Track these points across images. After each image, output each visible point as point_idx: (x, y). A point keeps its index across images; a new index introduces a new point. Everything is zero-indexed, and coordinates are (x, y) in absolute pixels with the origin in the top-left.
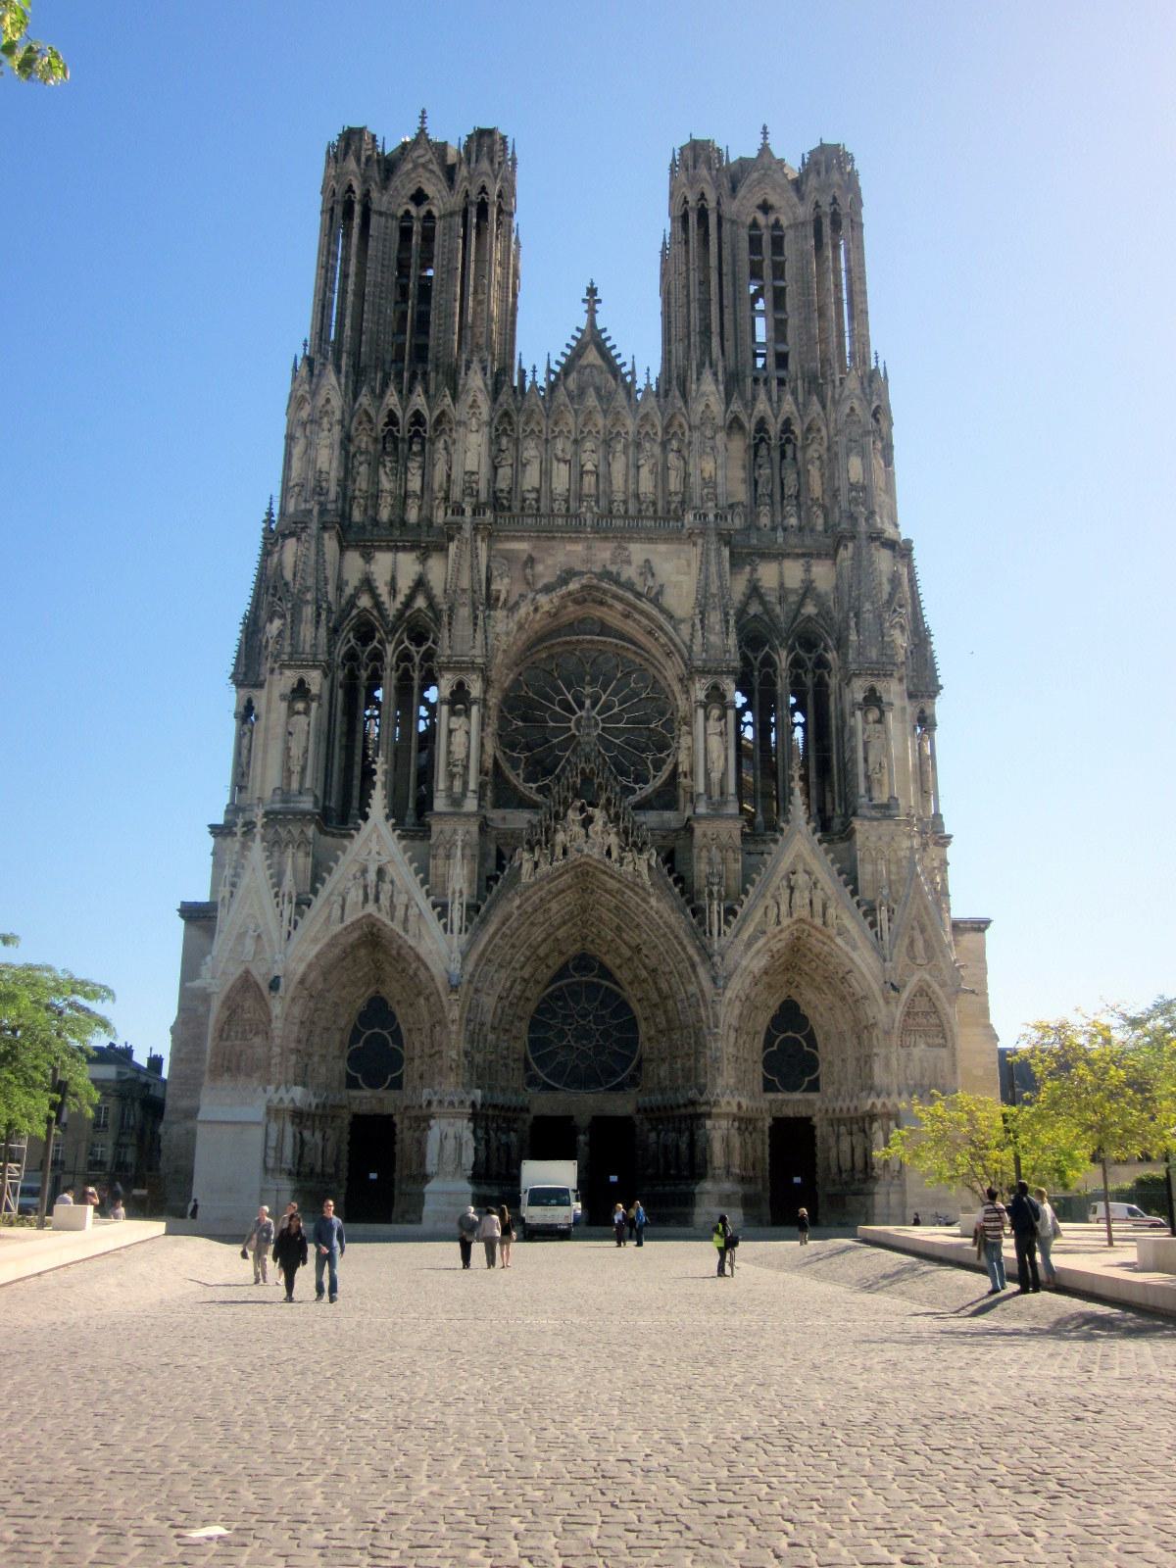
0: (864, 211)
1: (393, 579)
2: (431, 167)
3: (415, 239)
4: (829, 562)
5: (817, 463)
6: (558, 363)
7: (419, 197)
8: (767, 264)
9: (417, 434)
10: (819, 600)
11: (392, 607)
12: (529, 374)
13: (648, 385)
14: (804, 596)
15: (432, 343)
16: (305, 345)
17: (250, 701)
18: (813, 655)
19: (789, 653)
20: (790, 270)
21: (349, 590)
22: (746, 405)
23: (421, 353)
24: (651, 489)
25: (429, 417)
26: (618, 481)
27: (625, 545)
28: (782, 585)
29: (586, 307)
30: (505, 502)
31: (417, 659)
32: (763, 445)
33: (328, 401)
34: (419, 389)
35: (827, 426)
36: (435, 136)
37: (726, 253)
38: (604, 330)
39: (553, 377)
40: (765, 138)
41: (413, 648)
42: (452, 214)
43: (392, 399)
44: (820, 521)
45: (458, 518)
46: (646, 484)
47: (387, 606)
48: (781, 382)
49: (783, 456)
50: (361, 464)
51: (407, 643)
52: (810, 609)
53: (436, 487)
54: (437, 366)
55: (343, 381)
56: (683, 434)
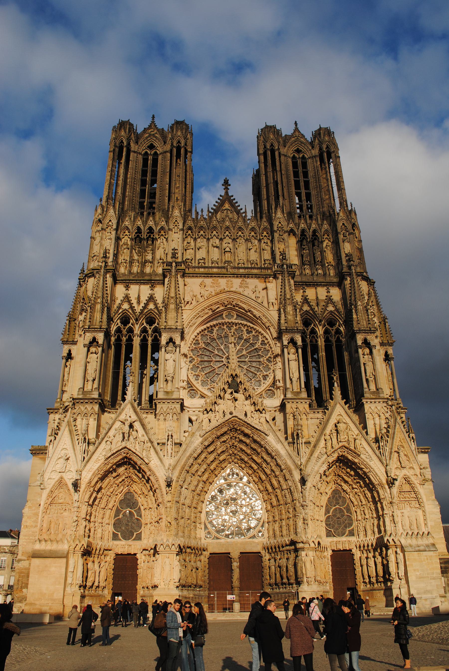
2: (156, 135)
6: (212, 209)
7: (151, 147)
12: (200, 213)
18: (334, 328)
19: (323, 328)
20: (311, 174)
22: (295, 224)
25: (156, 229)
28: (317, 298)
30: (190, 264)
31: (150, 332)
32: (305, 241)
33: (110, 221)
34: (151, 218)
37: (283, 166)
38: (232, 196)
39: (210, 214)
42: (165, 152)
43: (139, 223)
45: (169, 268)
48: (311, 217)
49: (314, 245)
50: (125, 249)
55: (117, 213)
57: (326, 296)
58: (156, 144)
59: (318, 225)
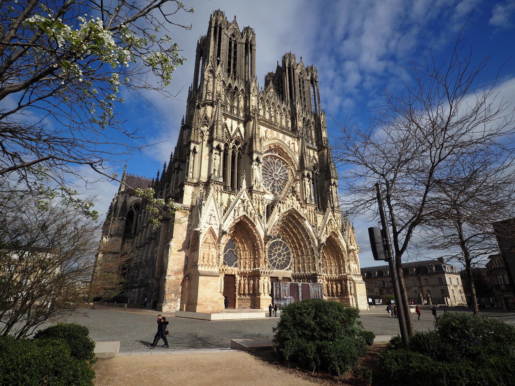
1: (232, 127)
31: (237, 149)
51: (234, 144)
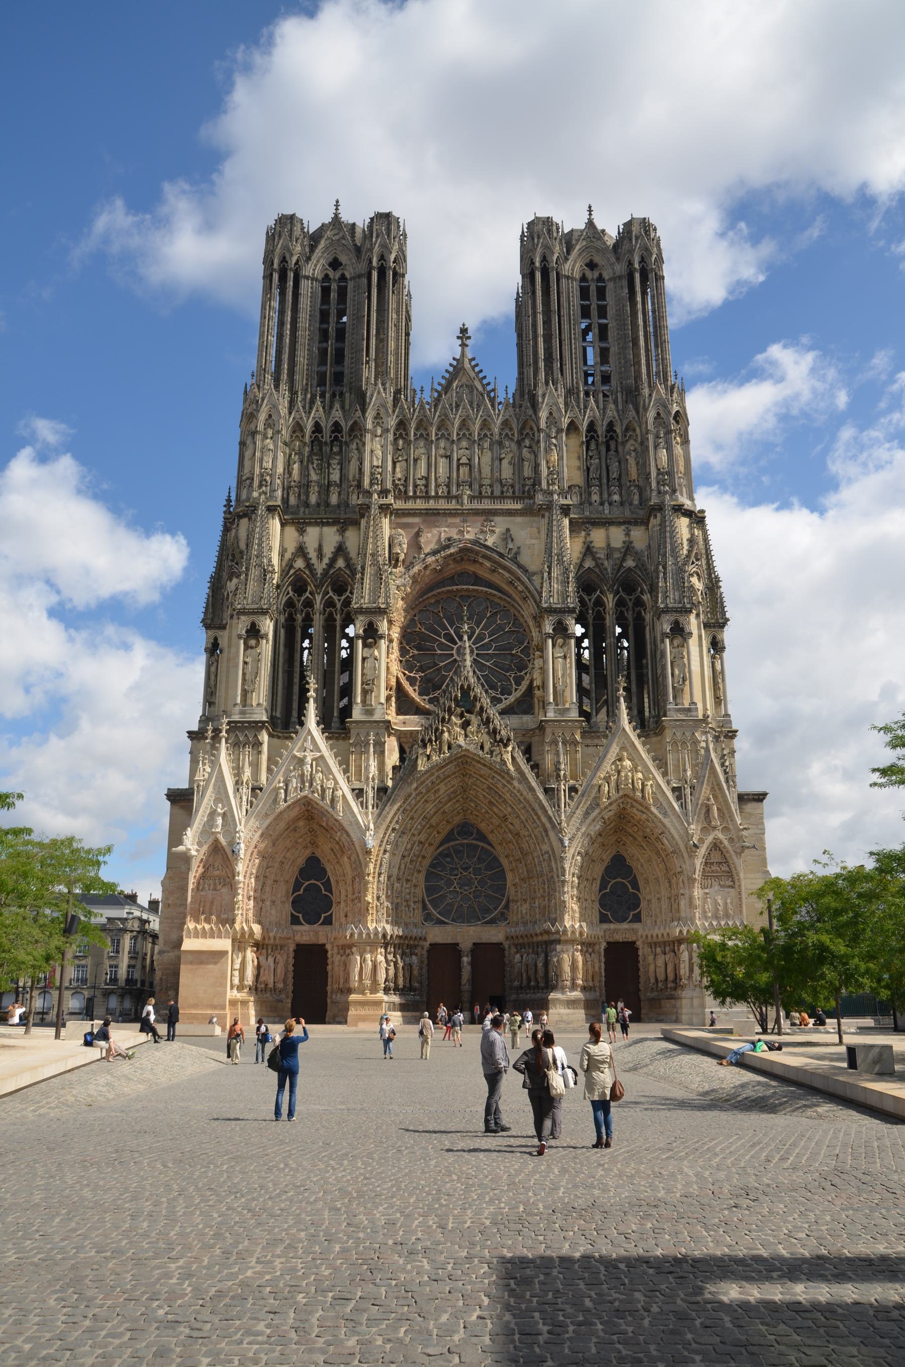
0: (664, 266)
1: (320, 550)
3: (334, 295)
4: (643, 528)
5: (633, 454)
6: (439, 384)
8: (594, 307)
9: (336, 437)
10: (637, 555)
11: (320, 567)
12: (418, 392)
13: (506, 399)
14: (625, 554)
15: (346, 371)
16: (253, 376)
17: (216, 639)
20: (611, 312)
21: (288, 556)
23: (338, 378)
24: (511, 476)
25: (345, 426)
26: (486, 471)
27: (491, 518)
28: (608, 545)
29: (460, 342)
31: (339, 606)
34: (337, 405)
35: (640, 427)
36: (347, 217)
40: (590, 215)
41: (336, 598)
42: (360, 276)
44: (636, 497)
46: (507, 472)
47: (316, 567)
49: (608, 449)
51: (331, 594)
52: (630, 563)
53: (351, 477)
54: (351, 389)
56: (533, 434)
57: (624, 542)
58: (343, 259)
59: (618, 411)
